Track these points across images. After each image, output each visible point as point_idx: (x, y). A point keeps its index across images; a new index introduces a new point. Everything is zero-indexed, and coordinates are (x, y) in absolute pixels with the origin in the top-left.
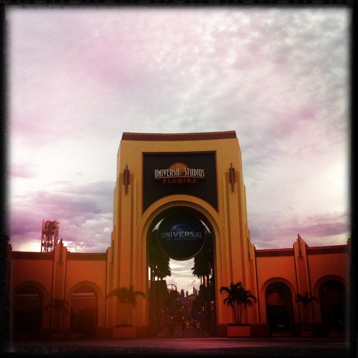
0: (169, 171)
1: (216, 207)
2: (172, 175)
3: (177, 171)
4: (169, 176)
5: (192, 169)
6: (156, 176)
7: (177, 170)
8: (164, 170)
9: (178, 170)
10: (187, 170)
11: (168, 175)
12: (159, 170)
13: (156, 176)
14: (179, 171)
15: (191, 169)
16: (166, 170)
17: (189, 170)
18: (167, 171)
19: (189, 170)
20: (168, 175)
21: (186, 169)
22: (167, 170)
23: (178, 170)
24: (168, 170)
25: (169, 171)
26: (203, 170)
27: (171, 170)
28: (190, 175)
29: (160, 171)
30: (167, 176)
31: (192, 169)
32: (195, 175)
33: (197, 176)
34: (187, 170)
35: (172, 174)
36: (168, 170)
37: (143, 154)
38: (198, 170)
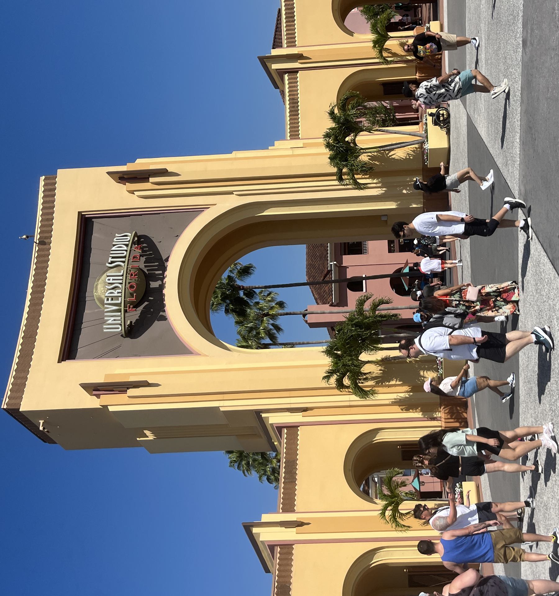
0: (110, 299)
1: (197, 211)
2: (120, 291)
3: (111, 281)
4: (121, 299)
5: (112, 252)
6: (118, 328)
7: (109, 282)
8: (106, 310)
9: (109, 280)
10: (112, 262)
11: (118, 300)
12: (104, 322)
13: (118, 328)
14: (111, 278)
15: (111, 255)
16: (106, 306)
17: (113, 258)
18: (110, 302)
19: (113, 258)
20: (118, 300)
21: (109, 263)
22: (106, 302)
23: (109, 280)
24: (108, 300)
25: (110, 299)
26: (117, 235)
27: (107, 295)
28: (125, 257)
29: (108, 320)
30: (119, 302)
31: (112, 252)
32: (125, 248)
33: (127, 245)
34: (112, 262)
35: (117, 291)
36: (108, 300)
37: (62, 360)
38: (114, 243)
